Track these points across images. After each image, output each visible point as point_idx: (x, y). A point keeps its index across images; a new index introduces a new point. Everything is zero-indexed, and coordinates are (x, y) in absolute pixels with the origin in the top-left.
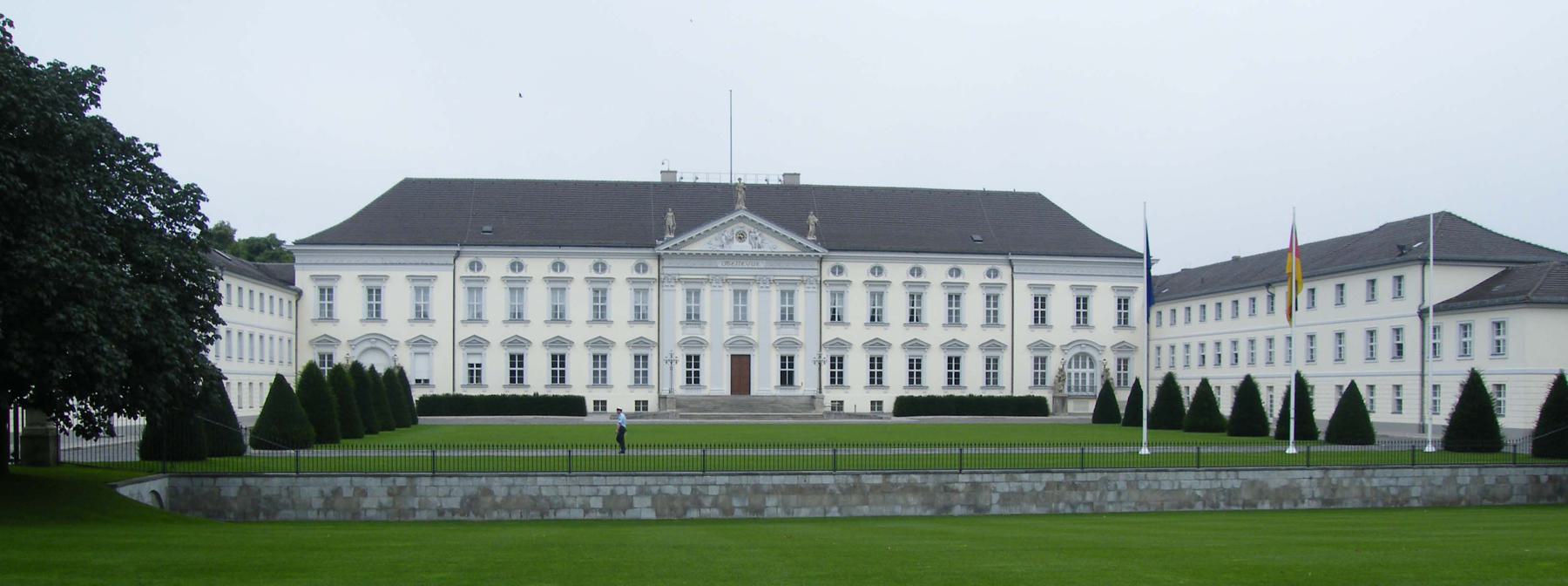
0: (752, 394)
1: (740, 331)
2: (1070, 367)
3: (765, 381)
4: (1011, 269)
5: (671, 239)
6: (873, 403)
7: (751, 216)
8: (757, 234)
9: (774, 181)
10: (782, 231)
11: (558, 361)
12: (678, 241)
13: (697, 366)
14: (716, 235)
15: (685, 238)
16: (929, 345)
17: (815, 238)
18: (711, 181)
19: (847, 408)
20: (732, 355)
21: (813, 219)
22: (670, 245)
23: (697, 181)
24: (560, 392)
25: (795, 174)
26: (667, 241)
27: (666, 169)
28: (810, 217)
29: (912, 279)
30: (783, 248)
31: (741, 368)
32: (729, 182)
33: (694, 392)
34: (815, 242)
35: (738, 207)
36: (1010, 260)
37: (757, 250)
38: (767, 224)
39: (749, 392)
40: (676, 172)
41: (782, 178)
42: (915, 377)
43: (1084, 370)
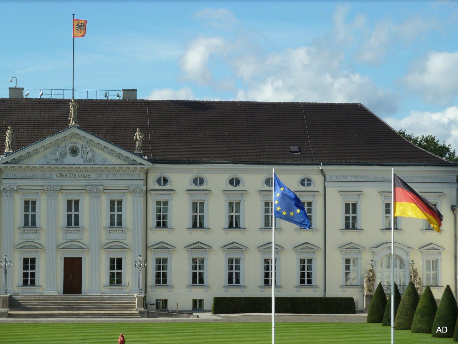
1: (73, 235)
4: (322, 178)
5: (10, 154)
6: (194, 301)
7: (82, 133)
8: (89, 149)
9: (113, 97)
10: (111, 147)
12: (16, 156)
13: (33, 268)
14: (51, 150)
15: (23, 152)
16: (246, 248)
17: (142, 152)
18: (56, 97)
19: (171, 306)
21: (138, 135)
22: (9, 159)
23: (42, 97)
25: (133, 90)
27: (14, 87)
28: (137, 133)
30: (113, 160)
32: (71, 98)
33: (29, 292)
34: (141, 156)
35: (72, 123)
36: (322, 170)
37: (87, 163)
38: (96, 140)
40: (23, 89)
41: (121, 94)
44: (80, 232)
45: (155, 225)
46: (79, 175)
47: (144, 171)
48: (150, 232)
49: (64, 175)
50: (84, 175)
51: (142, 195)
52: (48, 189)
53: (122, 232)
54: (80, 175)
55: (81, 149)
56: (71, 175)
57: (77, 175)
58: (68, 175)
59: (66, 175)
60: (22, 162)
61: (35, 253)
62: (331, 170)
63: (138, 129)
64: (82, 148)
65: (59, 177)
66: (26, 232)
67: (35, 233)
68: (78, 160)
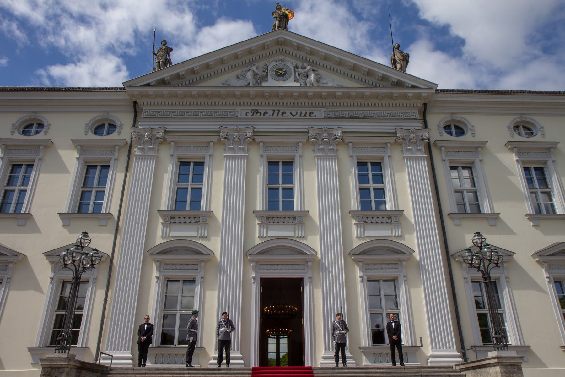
44: (297, 221)
46: (291, 113)
47: (420, 103)
48: (448, 223)
49: (262, 112)
50: (301, 112)
51: (422, 147)
52: (227, 135)
53: (389, 221)
54: (294, 113)
55: (295, 70)
56: (276, 112)
57: (288, 113)
58: (270, 113)
59: (265, 113)
61: (193, 267)
64: (296, 70)
65: (253, 115)
66: (177, 220)
67: (196, 222)
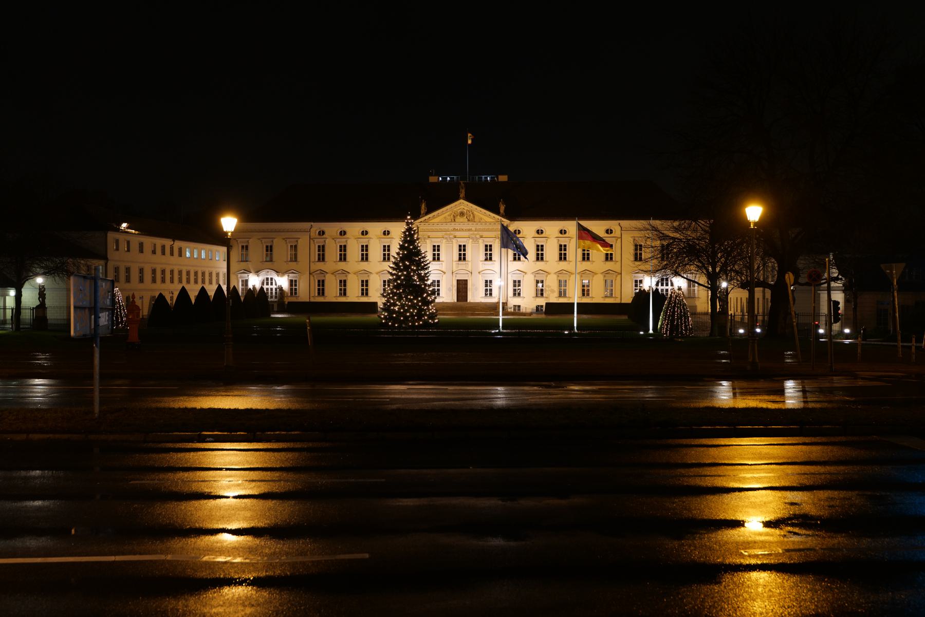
0: (468, 301)
2: (657, 285)
3: (476, 295)
4: (620, 228)
11: (365, 283)
15: (431, 215)
20: (457, 280)
24: (364, 299)
26: (422, 217)
29: (561, 235)
31: (462, 287)
34: (502, 216)
39: (467, 301)
42: (562, 294)
43: (667, 287)
45: (512, 259)
58: (459, 229)
60: (431, 221)
62: (626, 223)
63: (502, 200)
68: (464, 219)
